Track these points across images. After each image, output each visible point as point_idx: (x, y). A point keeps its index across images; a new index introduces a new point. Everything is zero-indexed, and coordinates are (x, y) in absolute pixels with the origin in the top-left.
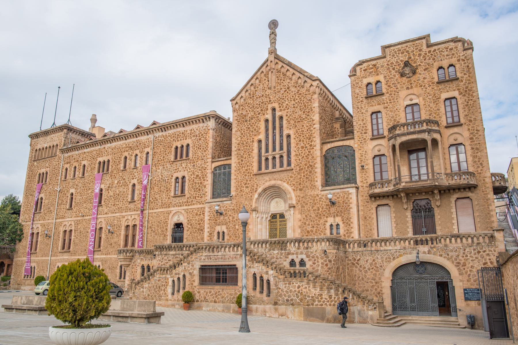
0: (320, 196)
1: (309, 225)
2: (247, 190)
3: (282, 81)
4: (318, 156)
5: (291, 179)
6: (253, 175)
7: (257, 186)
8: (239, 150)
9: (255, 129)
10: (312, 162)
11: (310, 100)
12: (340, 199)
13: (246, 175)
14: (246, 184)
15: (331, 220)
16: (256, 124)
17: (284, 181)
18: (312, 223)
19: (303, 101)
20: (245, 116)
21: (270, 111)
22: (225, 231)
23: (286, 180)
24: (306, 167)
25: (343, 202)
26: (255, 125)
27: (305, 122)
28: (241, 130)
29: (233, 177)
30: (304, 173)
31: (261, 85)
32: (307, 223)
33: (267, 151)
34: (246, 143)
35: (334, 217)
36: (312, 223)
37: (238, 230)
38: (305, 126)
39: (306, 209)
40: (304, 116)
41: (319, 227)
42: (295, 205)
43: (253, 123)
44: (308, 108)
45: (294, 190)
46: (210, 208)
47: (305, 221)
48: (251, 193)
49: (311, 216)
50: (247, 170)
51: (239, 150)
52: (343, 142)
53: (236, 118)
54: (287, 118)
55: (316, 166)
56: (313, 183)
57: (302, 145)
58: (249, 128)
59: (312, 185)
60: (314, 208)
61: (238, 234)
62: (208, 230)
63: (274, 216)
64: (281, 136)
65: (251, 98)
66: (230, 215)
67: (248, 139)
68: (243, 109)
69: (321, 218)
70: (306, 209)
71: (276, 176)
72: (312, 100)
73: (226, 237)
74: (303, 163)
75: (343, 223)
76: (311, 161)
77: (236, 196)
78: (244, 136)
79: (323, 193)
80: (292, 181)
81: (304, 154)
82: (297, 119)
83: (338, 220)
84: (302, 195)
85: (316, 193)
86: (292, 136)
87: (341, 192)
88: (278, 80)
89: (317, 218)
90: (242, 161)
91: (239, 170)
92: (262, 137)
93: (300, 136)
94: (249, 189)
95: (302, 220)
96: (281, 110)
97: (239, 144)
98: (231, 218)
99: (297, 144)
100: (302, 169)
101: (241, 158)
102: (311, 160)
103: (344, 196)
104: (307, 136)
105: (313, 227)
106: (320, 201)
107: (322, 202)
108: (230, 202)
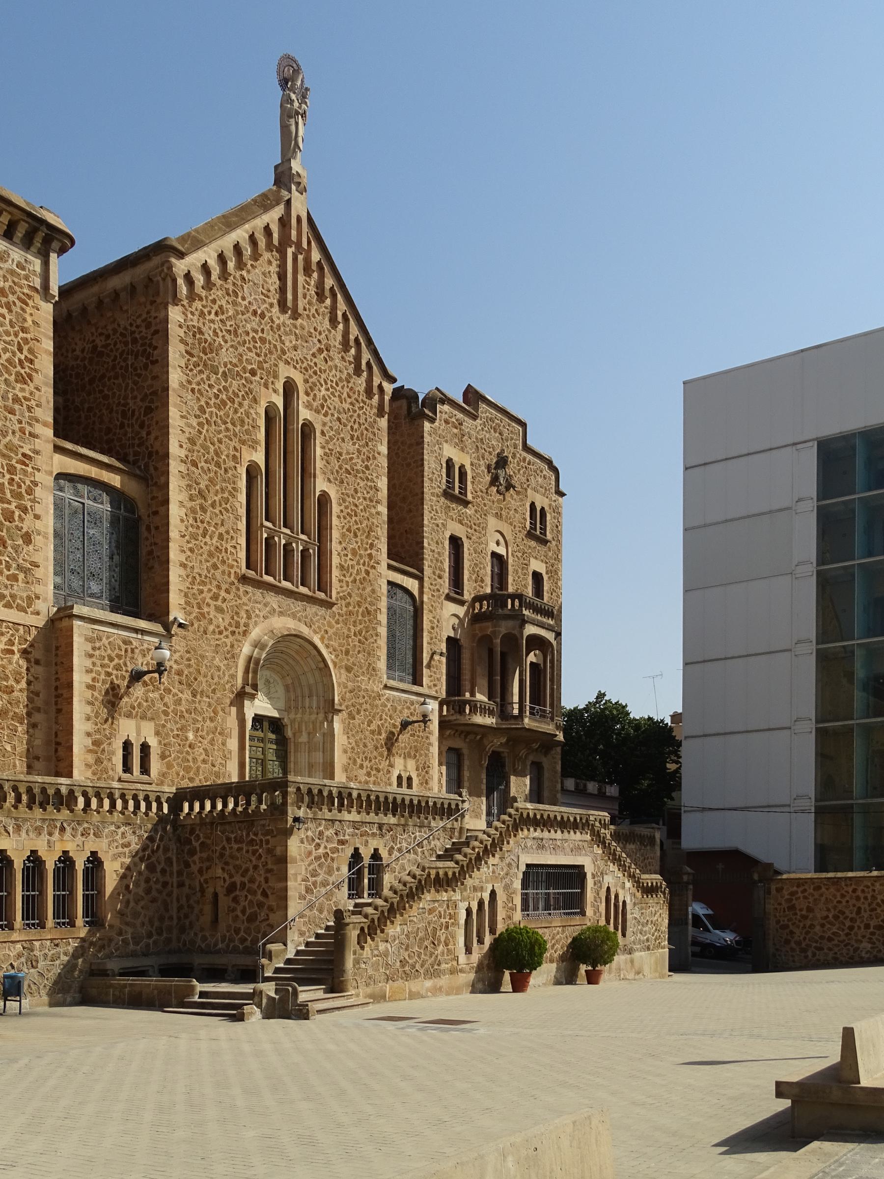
2: (222, 621)
7: (249, 617)
17: (315, 632)
48: (233, 633)
62: (89, 727)
66: (168, 691)
80: (330, 639)
92: (259, 457)
96: (309, 406)
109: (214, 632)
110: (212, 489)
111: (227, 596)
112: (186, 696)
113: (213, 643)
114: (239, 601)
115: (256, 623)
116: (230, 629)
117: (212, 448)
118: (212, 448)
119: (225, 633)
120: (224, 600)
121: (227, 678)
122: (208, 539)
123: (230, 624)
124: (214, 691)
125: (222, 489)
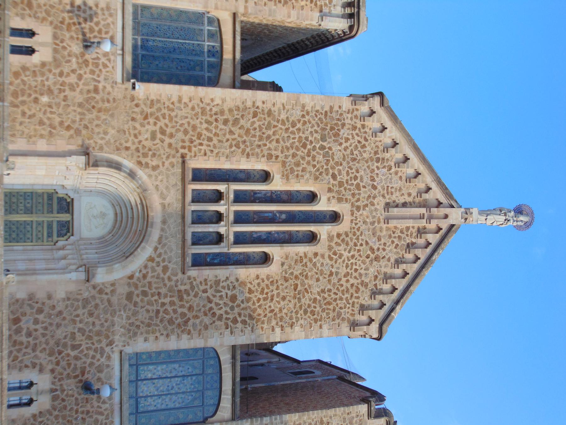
0: (107, 349)
1: (36, 322)
3: (396, 241)
4: (206, 341)
5: (159, 269)
6: (183, 156)
7: (155, 168)
8: (255, 115)
9: (298, 164)
10: (194, 325)
11: (339, 315)
12: (96, 404)
13: (186, 132)
14: (163, 132)
15: (43, 381)
16: (310, 168)
17: (156, 249)
18: (41, 331)
19: (341, 299)
20: (337, 135)
21: (335, 207)
22: (35, 58)
23: (160, 255)
24: (185, 310)
25: (88, 412)
26: (308, 163)
27: (291, 305)
28: (305, 123)
29: (187, 91)
30: (172, 303)
31: (400, 184)
32: (41, 317)
33: (240, 198)
34: (268, 137)
35: (52, 391)
36: (41, 331)
37: (36, 100)
38: (282, 303)
39: (80, 312)
40: (305, 301)
41: (29, 350)
42: (92, 282)
43: (314, 158)
44: (323, 310)
45: (131, 277)
46: (108, 8)
47: (46, 309)
48: (137, 150)
49: (58, 326)
50: (199, 136)
51: (255, 115)
52: (230, 392)
53: (336, 108)
54: (310, 255)
55: (185, 336)
56: (143, 329)
57: (240, 298)
58: (304, 146)
59: (138, 327)
60: (78, 336)
61: (23, 103)
63: (66, 205)
64: (269, 239)
65: (376, 153)
66: (80, 77)
67: (278, 141)
68: (354, 128)
69: (50, 355)
70: (80, 312)
71: (174, 227)
72: (337, 321)
73: (17, 60)
74: (195, 302)
75: (34, 416)
76: (198, 321)
77: (133, 99)
78: (287, 129)
79: (116, 357)
81: (217, 304)
82: (303, 284)
83: (43, 402)
84: (114, 300)
85: (117, 337)
86: (263, 271)
87: (112, 405)
88: (402, 232)
89: (52, 342)
90: (226, 122)
91: (203, 112)
92: (277, 184)
93: (262, 292)
94: (148, 144)
95: (50, 303)
96: (330, 238)
97: (270, 113)
98: (73, 79)
99: (243, 284)
100: (181, 299)
101: (233, 118)
102: (201, 322)
103: (101, 414)
104: (259, 311)
105: (29, 334)
106: (96, 350)
107: (93, 357)
108: (119, 79)
109: (135, 128)
110: (242, 132)
111: (166, 144)
112: (80, 99)
113: (126, 127)
114: (164, 157)
115: (150, 176)
116: (140, 147)
117: (270, 132)
118: (270, 132)
119: (136, 140)
120: (162, 141)
121: (100, 142)
122: (205, 125)
123: (144, 147)
124: (86, 127)
125: (244, 142)
